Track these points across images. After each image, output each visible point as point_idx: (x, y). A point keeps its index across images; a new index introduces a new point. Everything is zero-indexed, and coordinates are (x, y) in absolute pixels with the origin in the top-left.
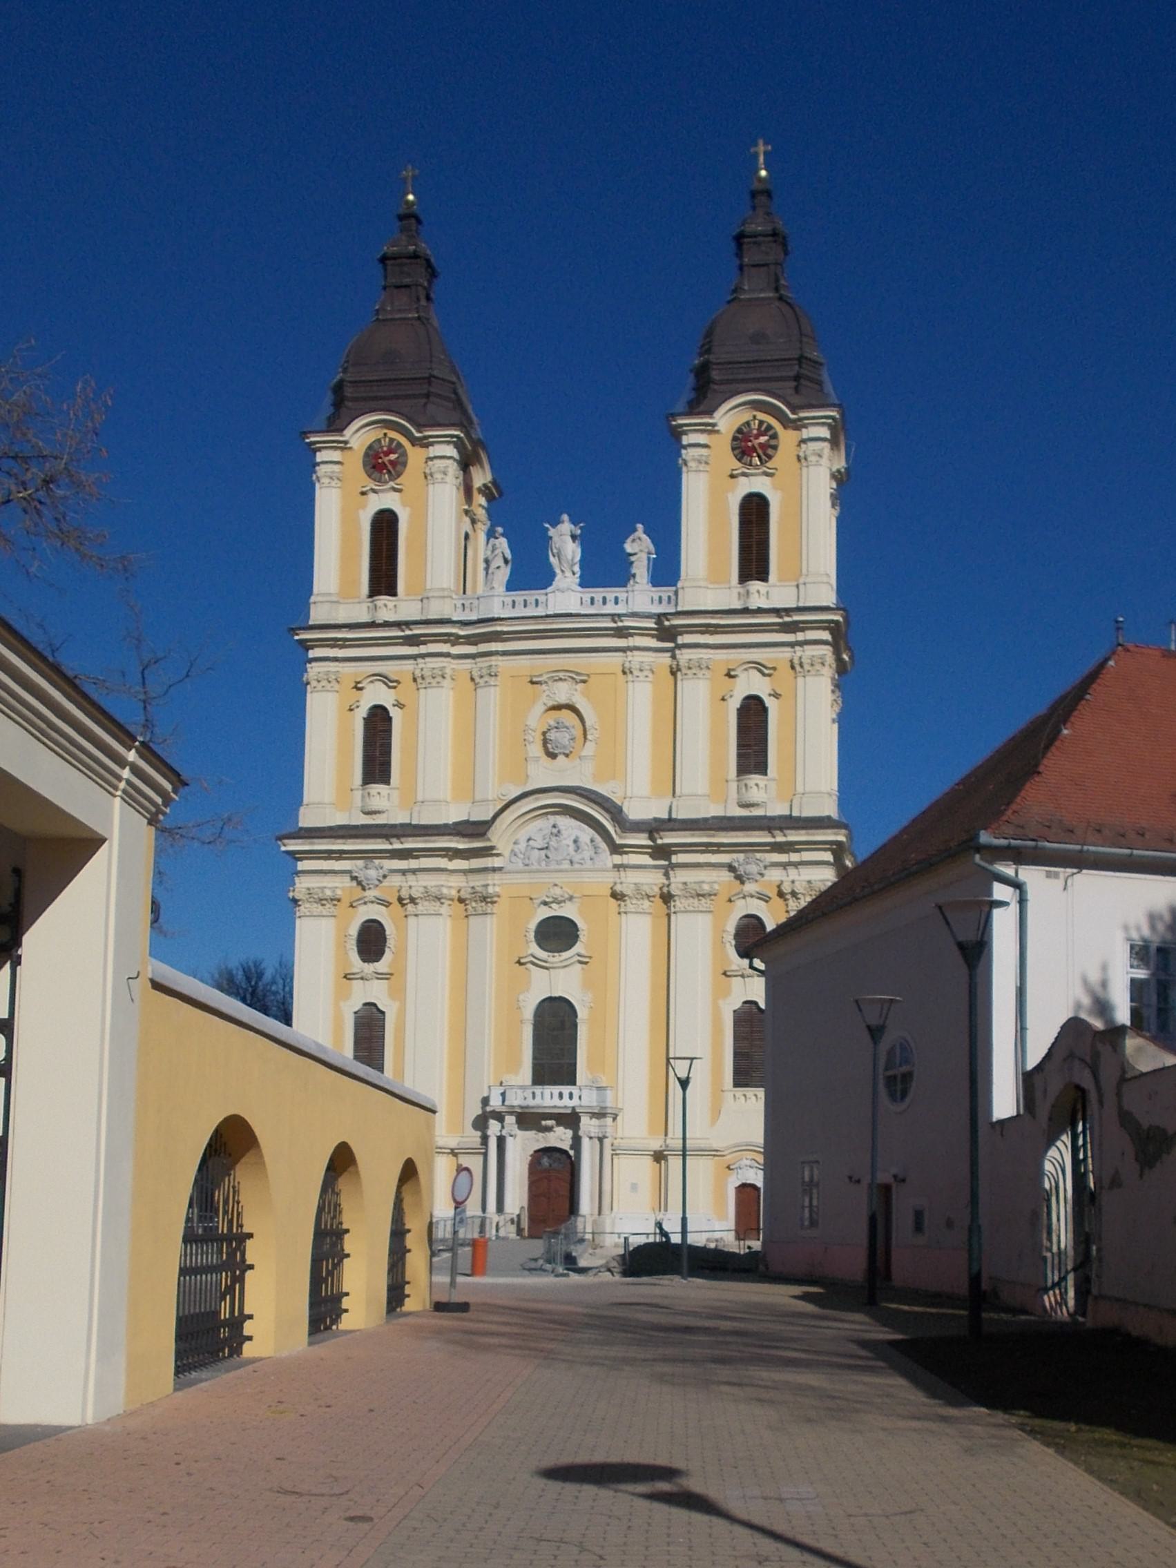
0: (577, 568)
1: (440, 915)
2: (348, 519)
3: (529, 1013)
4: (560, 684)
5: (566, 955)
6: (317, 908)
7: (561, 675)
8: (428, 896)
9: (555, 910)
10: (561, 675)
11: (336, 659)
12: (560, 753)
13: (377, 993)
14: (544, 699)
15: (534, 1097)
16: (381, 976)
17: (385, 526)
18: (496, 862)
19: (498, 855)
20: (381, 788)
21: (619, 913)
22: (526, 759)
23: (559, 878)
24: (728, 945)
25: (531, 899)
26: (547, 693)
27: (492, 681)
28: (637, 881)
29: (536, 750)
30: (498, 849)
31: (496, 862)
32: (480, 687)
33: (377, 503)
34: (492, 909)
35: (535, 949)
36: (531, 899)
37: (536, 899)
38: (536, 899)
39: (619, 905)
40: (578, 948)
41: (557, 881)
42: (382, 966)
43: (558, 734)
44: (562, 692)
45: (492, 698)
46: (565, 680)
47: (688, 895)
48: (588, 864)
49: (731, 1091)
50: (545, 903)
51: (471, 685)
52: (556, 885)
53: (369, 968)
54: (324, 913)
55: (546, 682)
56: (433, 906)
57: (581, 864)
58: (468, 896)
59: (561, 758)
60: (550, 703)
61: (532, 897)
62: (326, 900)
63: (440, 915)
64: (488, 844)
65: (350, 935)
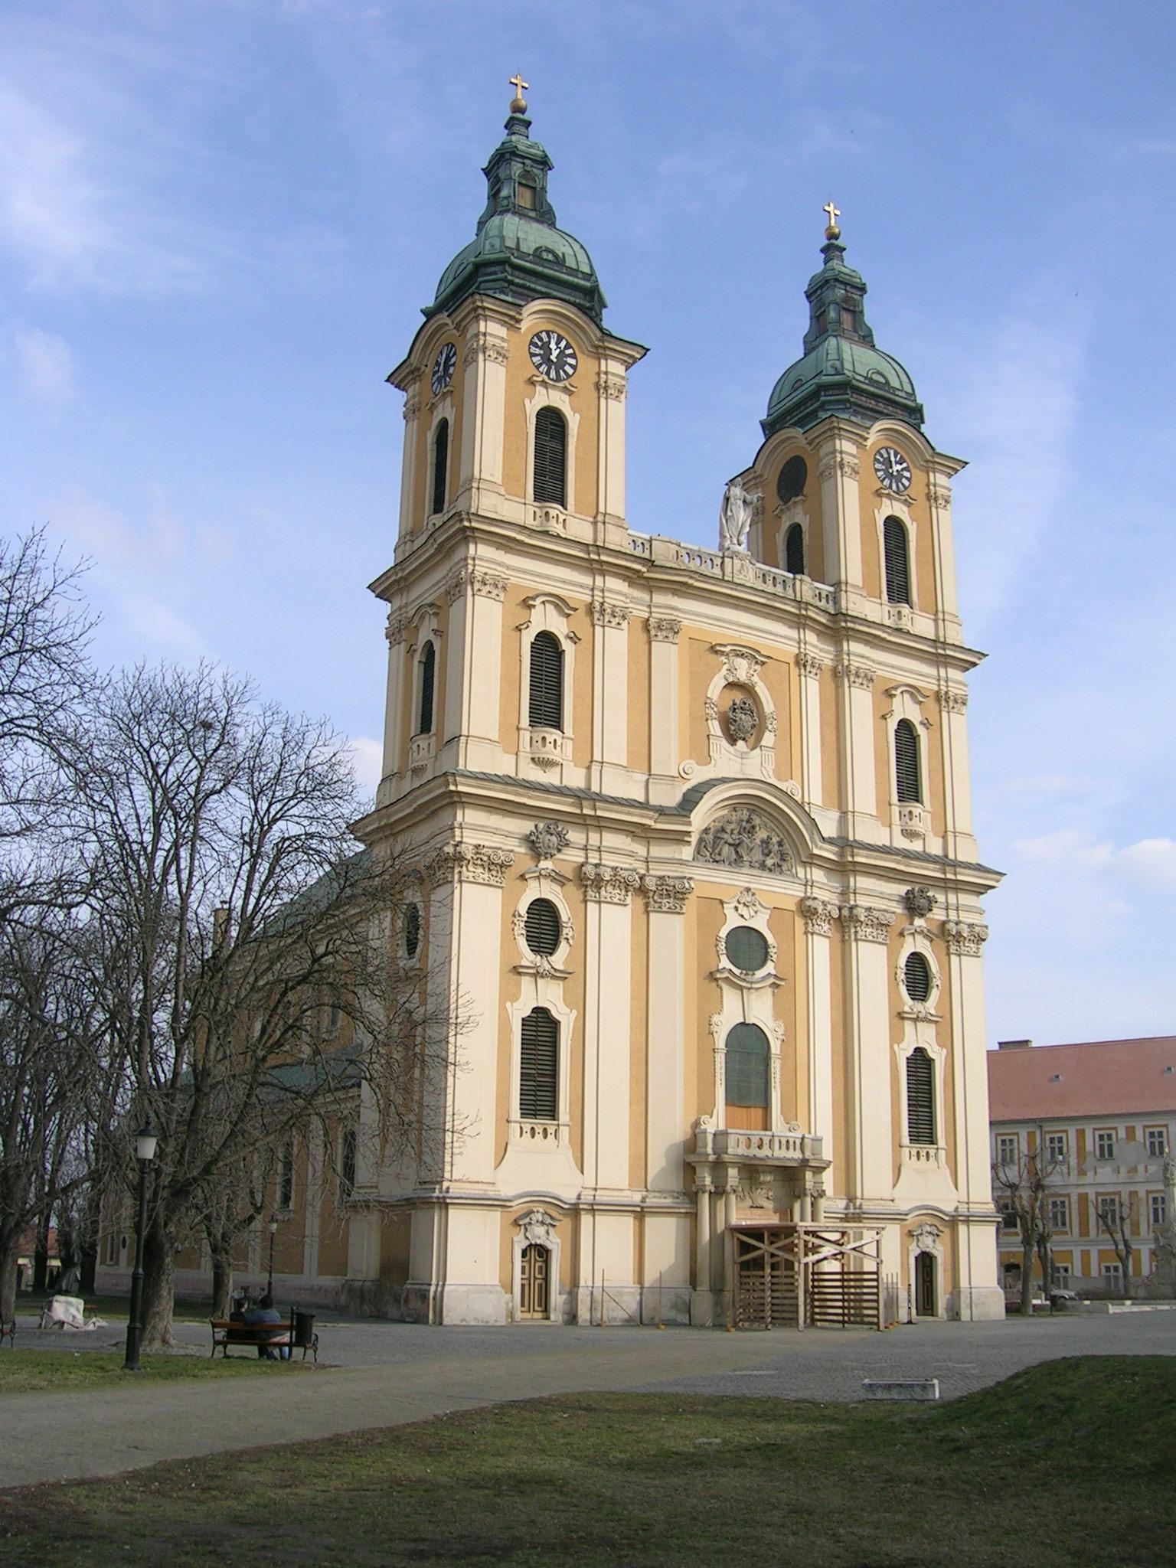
0: (743, 538)
3: (721, 1042)
4: (739, 660)
6: (482, 875)
10: (744, 650)
13: (552, 997)
14: (724, 671)
15: (760, 1147)
17: (551, 424)
20: (552, 734)
21: (806, 933)
24: (901, 983)
29: (715, 727)
33: (543, 398)
35: (725, 963)
39: (807, 923)
40: (769, 968)
41: (751, 886)
43: (743, 717)
45: (667, 656)
47: (870, 923)
51: (644, 636)
52: (748, 890)
56: (616, 894)
58: (654, 888)
60: (731, 679)
62: (496, 865)
63: (626, 905)
65: (520, 916)
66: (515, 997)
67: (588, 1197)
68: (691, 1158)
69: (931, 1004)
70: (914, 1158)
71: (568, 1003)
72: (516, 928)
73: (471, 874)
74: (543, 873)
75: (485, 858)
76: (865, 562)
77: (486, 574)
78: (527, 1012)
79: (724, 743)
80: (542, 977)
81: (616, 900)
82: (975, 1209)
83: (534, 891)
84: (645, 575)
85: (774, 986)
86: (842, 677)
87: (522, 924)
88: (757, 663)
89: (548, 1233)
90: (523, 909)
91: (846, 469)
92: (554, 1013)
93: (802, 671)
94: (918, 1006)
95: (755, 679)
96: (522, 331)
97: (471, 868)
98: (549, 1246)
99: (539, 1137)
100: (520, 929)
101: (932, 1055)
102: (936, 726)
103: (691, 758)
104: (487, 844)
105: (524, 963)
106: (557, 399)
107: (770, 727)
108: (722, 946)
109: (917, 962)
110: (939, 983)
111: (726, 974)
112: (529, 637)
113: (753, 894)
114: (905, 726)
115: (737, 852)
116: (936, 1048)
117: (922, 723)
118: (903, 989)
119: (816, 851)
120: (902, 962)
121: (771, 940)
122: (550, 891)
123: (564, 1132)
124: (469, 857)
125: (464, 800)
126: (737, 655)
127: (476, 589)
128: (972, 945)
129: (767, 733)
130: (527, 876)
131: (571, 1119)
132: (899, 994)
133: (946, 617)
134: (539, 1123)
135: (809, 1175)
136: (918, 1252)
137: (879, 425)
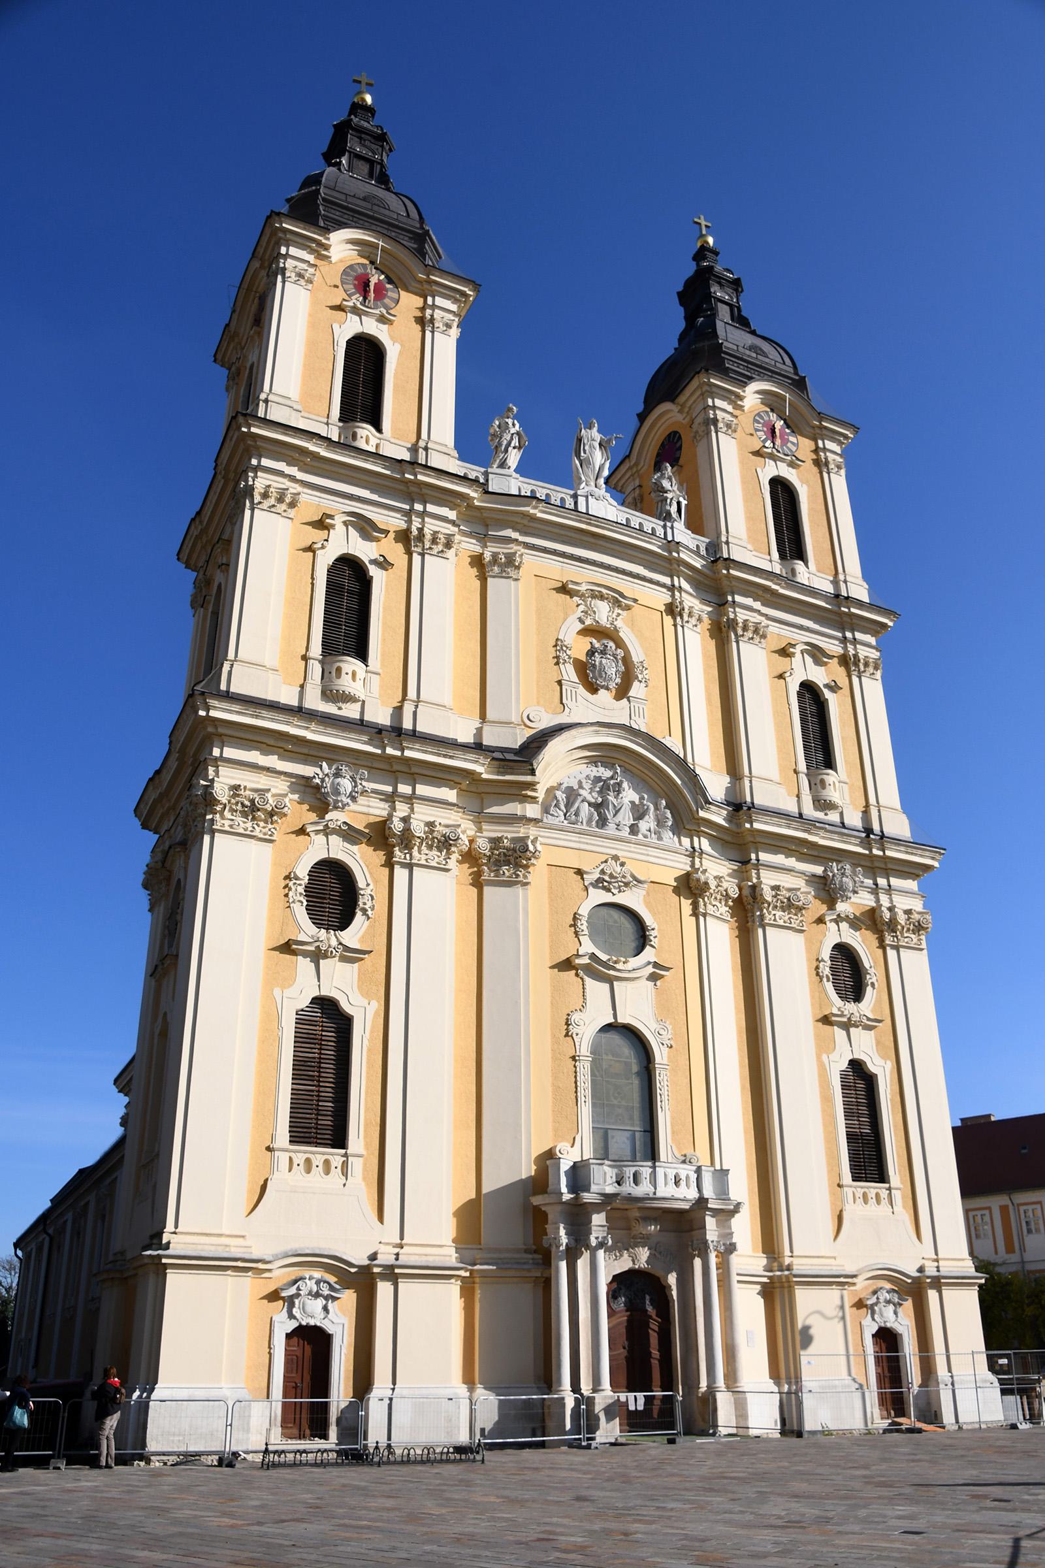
1: (448, 870)
2: (317, 330)
5: (634, 962)
7: (604, 591)
8: (434, 838)
9: (614, 894)
10: (604, 591)
11: (292, 478)
12: (602, 687)
16: (350, 955)
18: (532, 811)
19: (533, 799)
22: (560, 683)
23: (622, 850)
25: (580, 872)
26: (582, 608)
27: (513, 573)
28: (721, 875)
30: (535, 790)
31: (532, 811)
32: (494, 577)
34: (525, 877)
35: (588, 946)
36: (580, 872)
37: (587, 873)
38: (587, 873)
40: (648, 954)
41: (620, 854)
42: (352, 936)
43: (604, 661)
44: (603, 613)
46: (607, 599)
48: (653, 839)
49: (851, 1186)
50: (599, 883)
52: (615, 858)
53: (328, 938)
54: (257, 833)
55: (582, 596)
57: (645, 836)
59: (602, 692)
60: (588, 622)
61: (585, 869)
63: (448, 870)
64: (529, 778)
65: (297, 878)
66: (289, 980)
67: (386, 1257)
68: (536, 1200)
69: (868, 1006)
70: (860, 1201)
71: (366, 994)
72: (291, 894)
73: (227, 823)
74: (331, 825)
75: (247, 803)
76: (750, 518)
77: (269, 486)
78: (304, 1002)
79: (581, 690)
80: (325, 957)
81: (434, 864)
82: (947, 1268)
83: (318, 849)
84: (476, 503)
85: (653, 978)
86: (728, 632)
87: (301, 889)
88: (619, 607)
89: (325, 1309)
90: (303, 872)
91: (720, 425)
92: (345, 1006)
93: (678, 619)
94: (851, 1008)
95: (619, 623)
96: (333, 260)
97: (227, 814)
98: (329, 1328)
99: (317, 1171)
100: (298, 891)
101: (872, 1068)
102: (846, 691)
103: (538, 703)
104: (249, 785)
105: (302, 937)
106: (371, 327)
107: (640, 677)
108: (583, 925)
109: (844, 952)
110: (874, 980)
111: (586, 960)
112: (326, 559)
113: (622, 864)
114: (809, 690)
115: (599, 814)
116: (878, 1060)
117: (827, 686)
118: (829, 987)
119: (702, 814)
120: (826, 953)
121: (649, 920)
122: (339, 850)
123: (356, 1165)
124: (224, 801)
125: (221, 730)
126: (593, 597)
127: (256, 501)
128: (913, 936)
129: (636, 684)
130: (309, 829)
131: (367, 1146)
132: (824, 990)
133: (848, 578)
134: (319, 1154)
135: (710, 1222)
136: (875, 1329)
137: (754, 386)
